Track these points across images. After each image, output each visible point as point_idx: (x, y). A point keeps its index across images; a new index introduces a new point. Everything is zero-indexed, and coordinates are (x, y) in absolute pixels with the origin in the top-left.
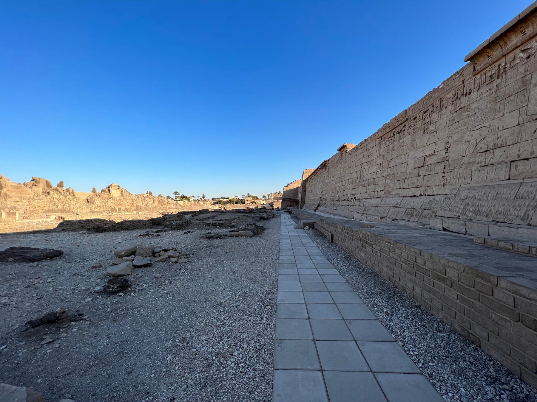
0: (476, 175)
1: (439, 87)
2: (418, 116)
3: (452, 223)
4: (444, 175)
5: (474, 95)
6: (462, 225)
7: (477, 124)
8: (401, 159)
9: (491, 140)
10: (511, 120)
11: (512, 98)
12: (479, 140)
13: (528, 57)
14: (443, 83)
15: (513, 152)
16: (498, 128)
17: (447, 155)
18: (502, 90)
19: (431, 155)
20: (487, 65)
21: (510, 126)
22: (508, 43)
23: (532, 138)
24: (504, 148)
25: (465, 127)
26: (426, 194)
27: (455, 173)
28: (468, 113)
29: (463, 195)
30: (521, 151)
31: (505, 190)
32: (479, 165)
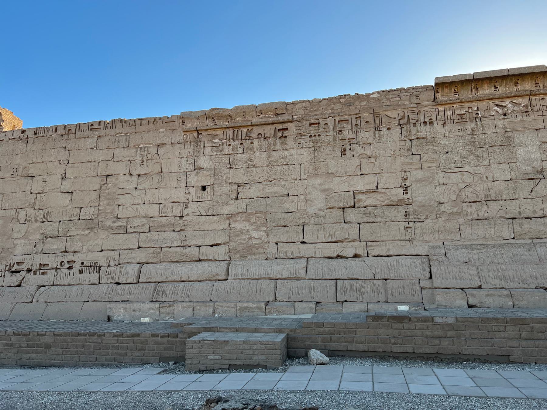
0: (467, 231)
1: (369, 95)
2: (322, 123)
3: (487, 295)
4: (407, 225)
5: (438, 128)
6: (507, 296)
7: (453, 165)
8: (284, 186)
9: (481, 189)
10: (502, 173)
11: (496, 149)
12: (462, 186)
13: (505, 115)
14: (379, 92)
15: (513, 208)
16: (487, 177)
17: (406, 196)
18: (481, 136)
19: (368, 192)
20: (458, 101)
21: (502, 179)
22: (479, 89)
23: (530, 197)
24: (501, 202)
25: (434, 165)
26: (372, 253)
27: (431, 224)
28: (434, 148)
29: (460, 255)
30: (522, 209)
31: (520, 250)
32: (470, 218)
